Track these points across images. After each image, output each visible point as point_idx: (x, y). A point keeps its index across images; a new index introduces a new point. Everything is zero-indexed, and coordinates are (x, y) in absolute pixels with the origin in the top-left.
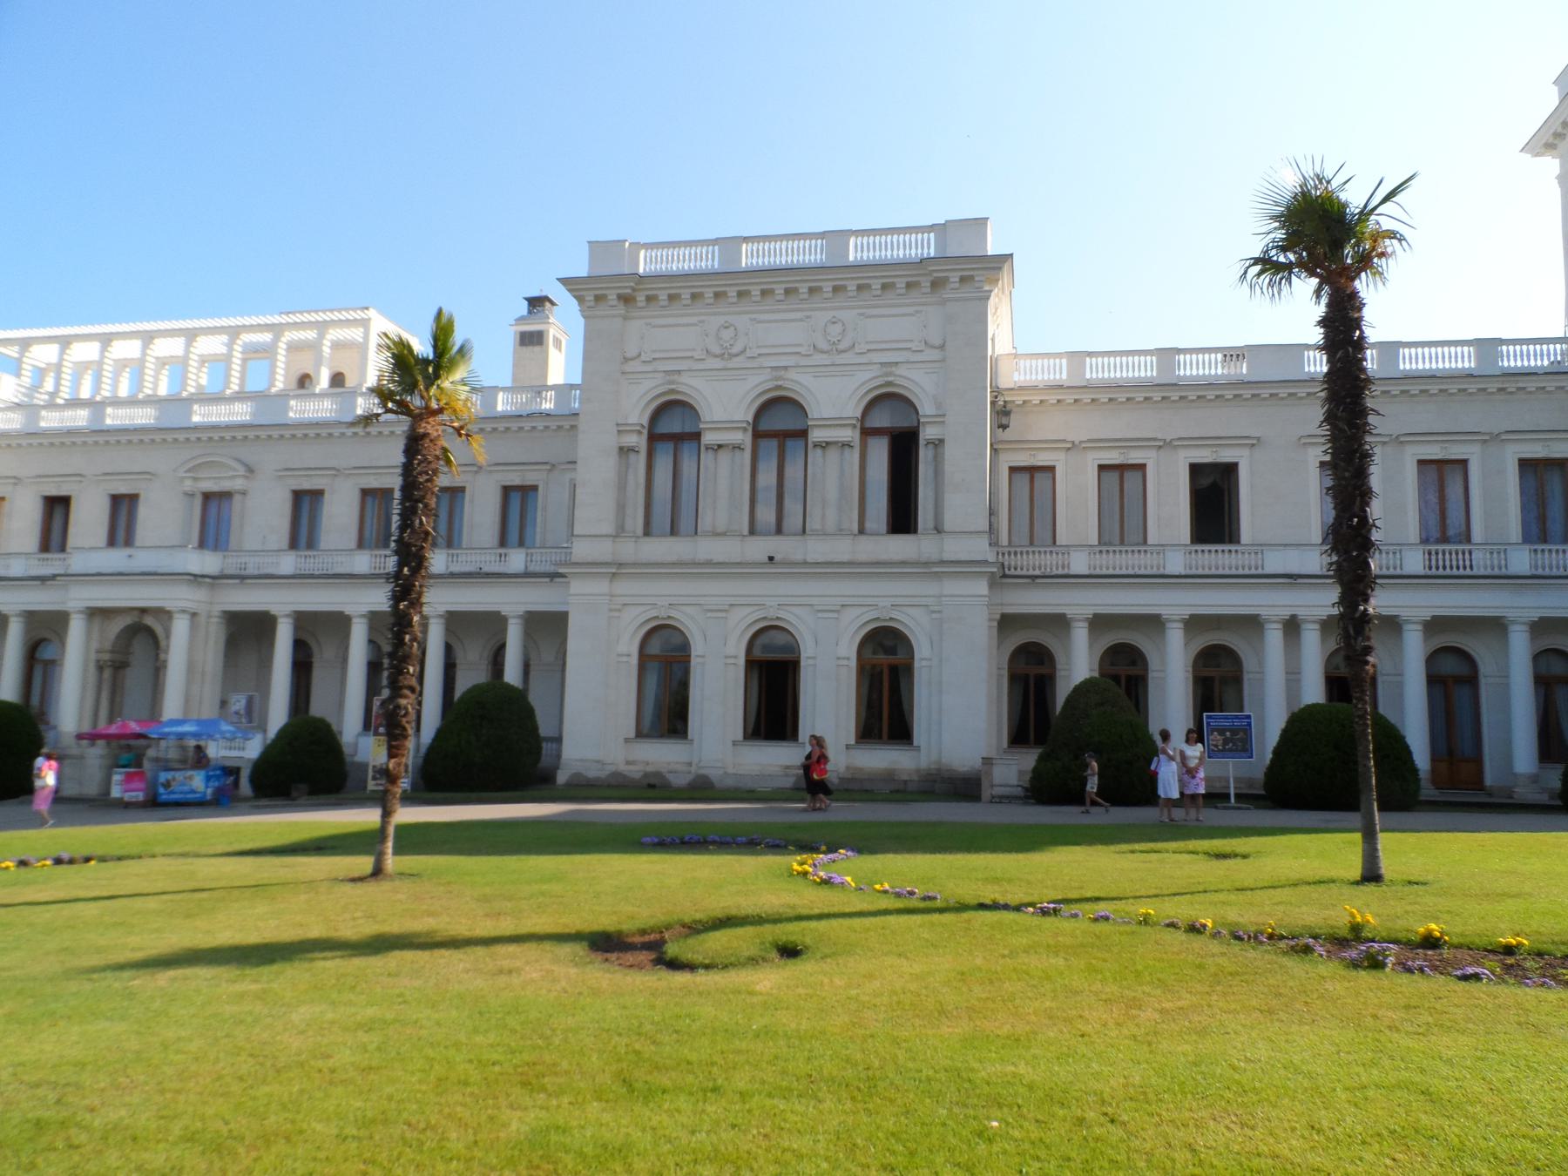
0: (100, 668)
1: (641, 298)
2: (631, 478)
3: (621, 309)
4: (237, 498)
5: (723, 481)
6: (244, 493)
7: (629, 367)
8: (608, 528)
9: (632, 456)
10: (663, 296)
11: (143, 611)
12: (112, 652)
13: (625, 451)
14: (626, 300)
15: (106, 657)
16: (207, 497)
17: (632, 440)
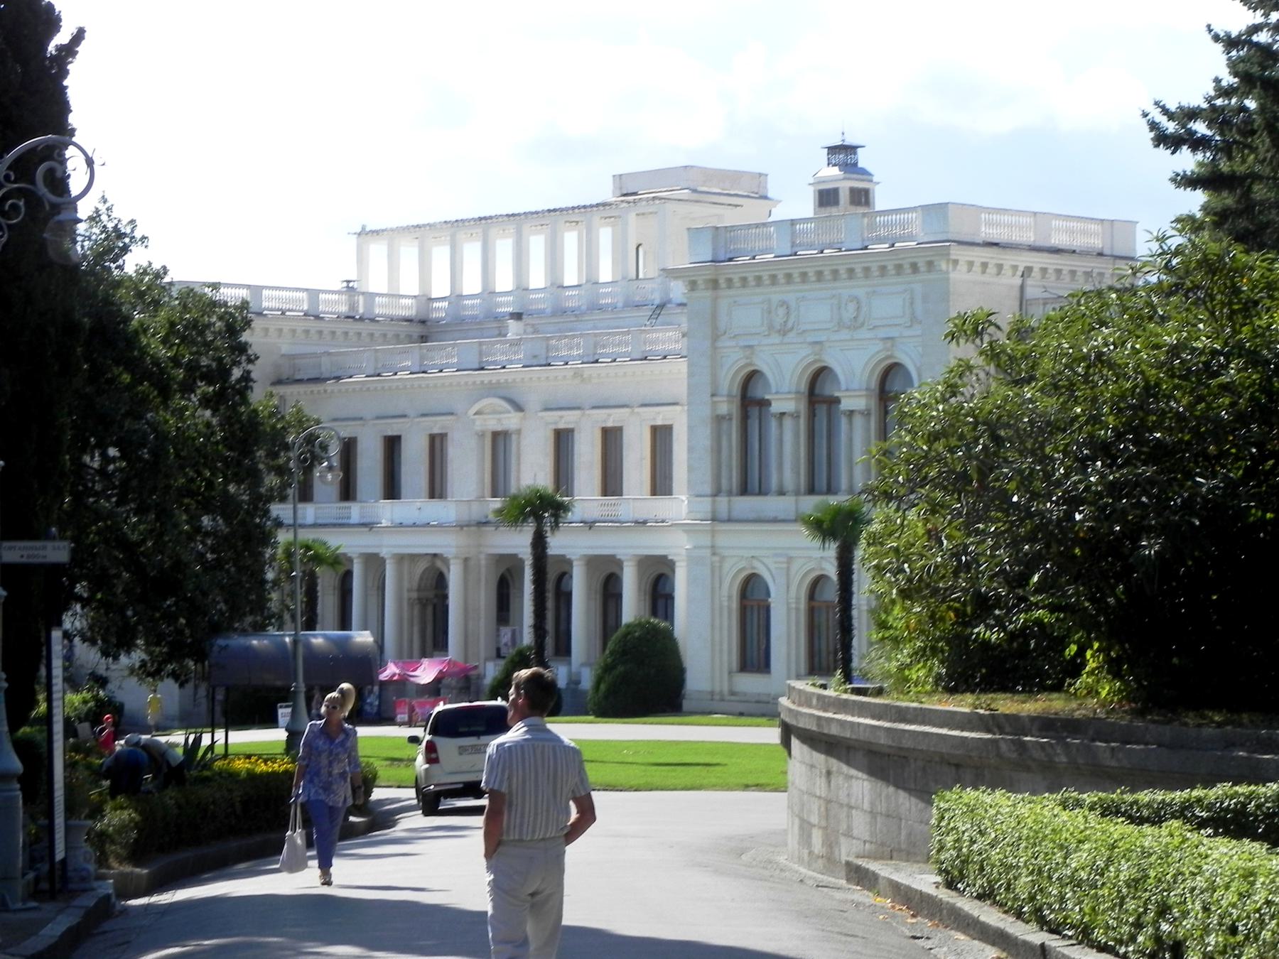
0: (411, 606)
1: (722, 281)
2: (724, 443)
3: (708, 293)
4: (514, 437)
5: (786, 448)
6: (519, 432)
7: (719, 344)
8: (708, 489)
9: (725, 426)
10: (736, 278)
11: (435, 555)
12: (419, 590)
13: (719, 420)
14: (714, 284)
15: (415, 595)
16: (495, 435)
17: (724, 409)
